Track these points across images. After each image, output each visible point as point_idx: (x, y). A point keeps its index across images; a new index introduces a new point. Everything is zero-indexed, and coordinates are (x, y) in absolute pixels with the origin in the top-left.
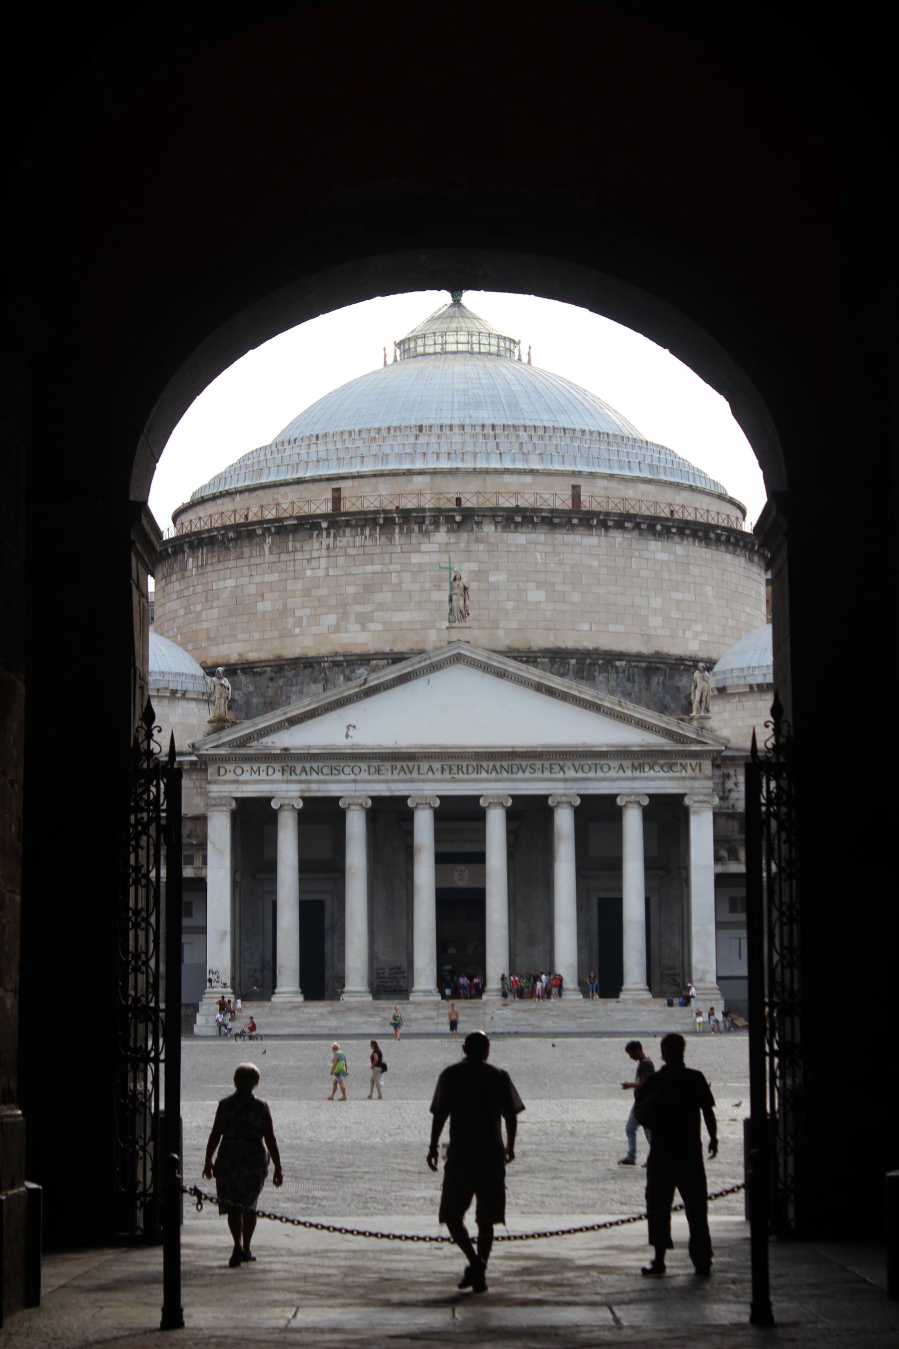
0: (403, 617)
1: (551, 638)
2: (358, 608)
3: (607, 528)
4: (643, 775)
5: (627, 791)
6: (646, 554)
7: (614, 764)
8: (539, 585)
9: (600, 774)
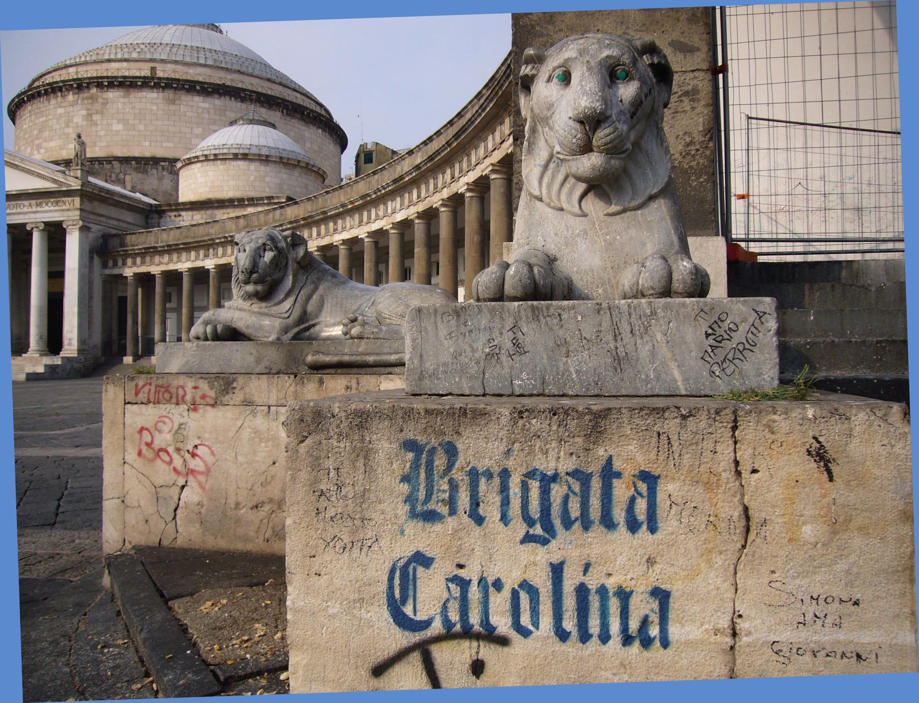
0: (52, 144)
1: (125, 151)
2: (37, 142)
3: (164, 88)
4: (42, 209)
5: (33, 220)
6: (191, 103)
7: (26, 203)
8: (119, 121)
9: (19, 210)
